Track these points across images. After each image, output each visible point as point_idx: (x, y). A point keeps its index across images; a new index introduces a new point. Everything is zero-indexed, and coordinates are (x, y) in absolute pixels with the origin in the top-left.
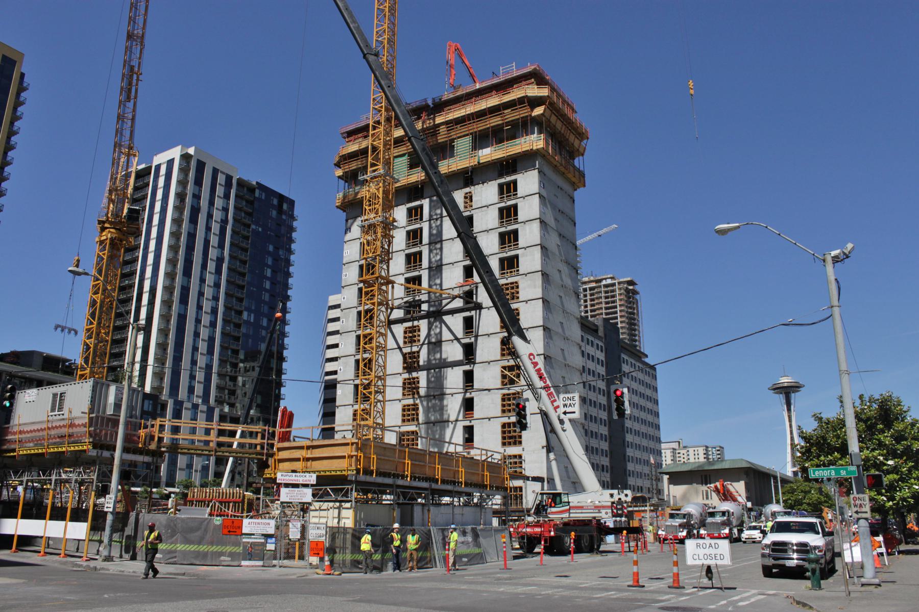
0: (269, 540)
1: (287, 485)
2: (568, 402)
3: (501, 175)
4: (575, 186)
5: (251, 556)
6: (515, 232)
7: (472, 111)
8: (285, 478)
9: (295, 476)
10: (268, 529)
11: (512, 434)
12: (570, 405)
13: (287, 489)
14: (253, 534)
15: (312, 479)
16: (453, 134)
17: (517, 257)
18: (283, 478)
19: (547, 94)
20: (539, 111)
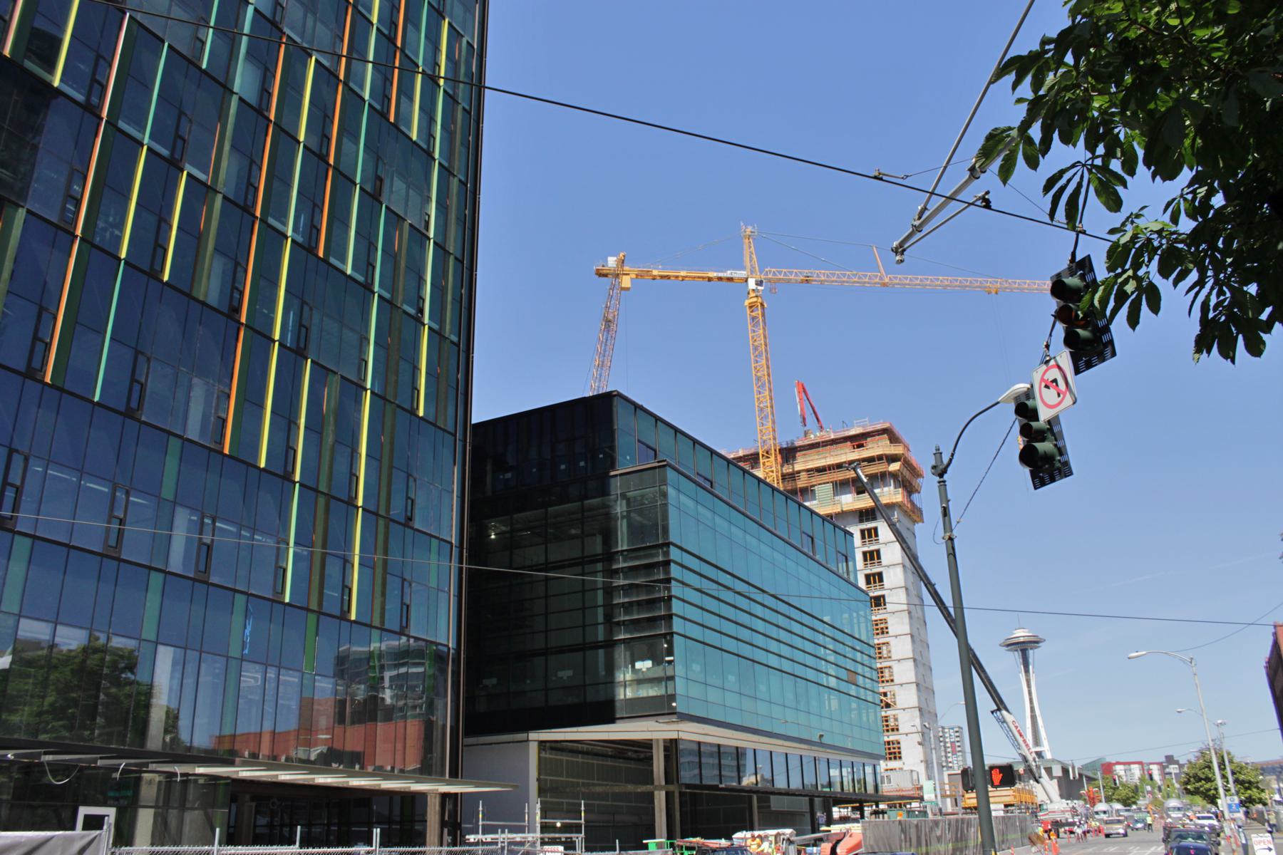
3: (861, 521)
4: (914, 522)
6: (880, 575)
7: (832, 462)
11: (892, 750)
16: (813, 481)
17: (883, 596)
19: (901, 452)
20: (895, 467)
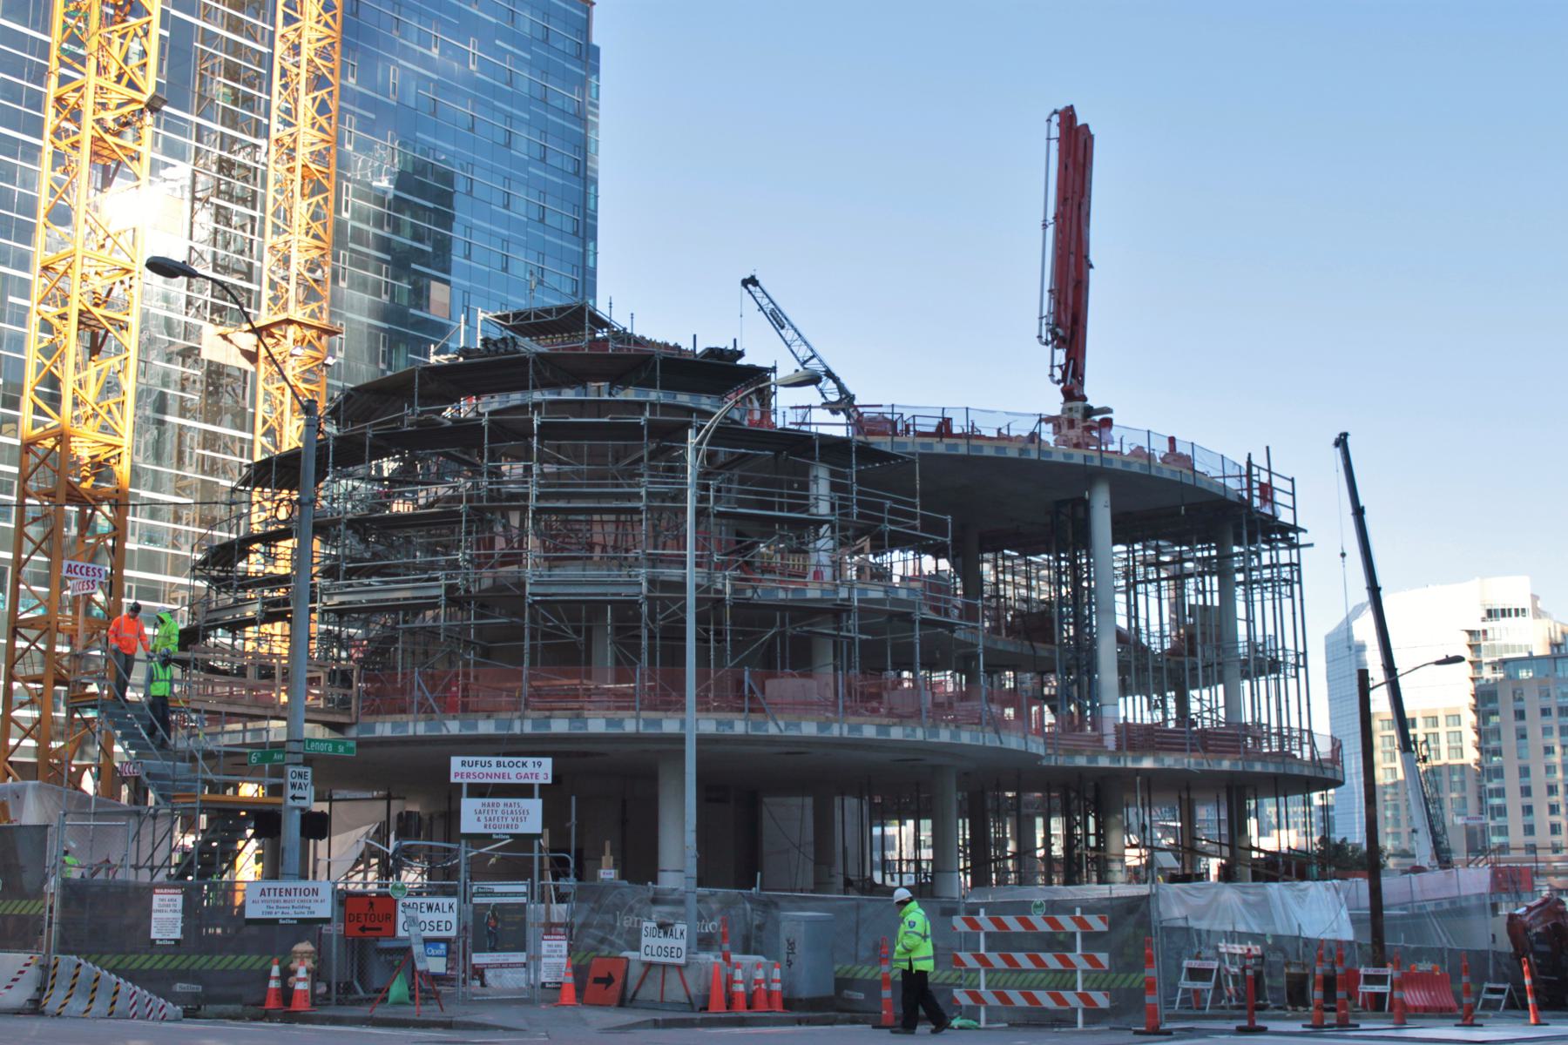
1: (478, 791)
8: (471, 770)
9: (498, 764)
15: (541, 770)
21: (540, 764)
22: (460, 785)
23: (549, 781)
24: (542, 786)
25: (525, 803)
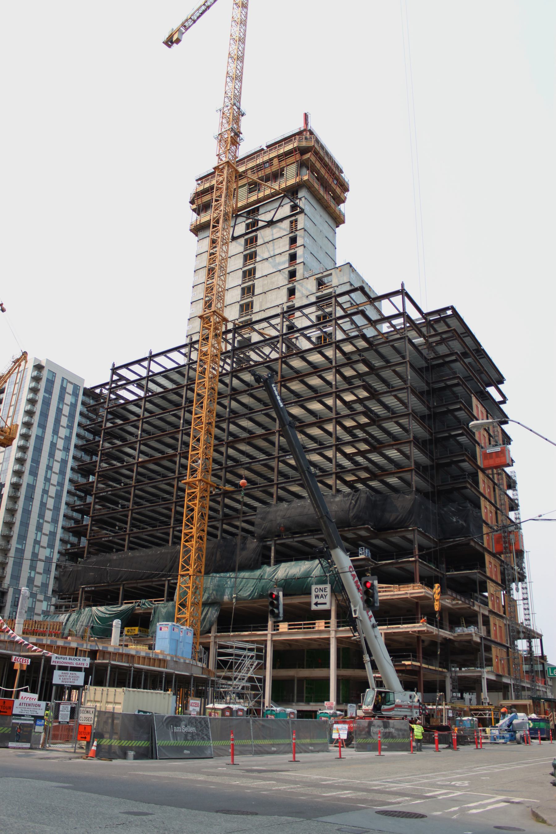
0: (38, 722)
1: (62, 668)
2: (320, 593)
5: (19, 737)
9: (70, 659)
10: (38, 711)
12: (322, 596)
13: (61, 672)
14: (23, 716)
18: (57, 660)
21: (85, 660)
22: (55, 666)
23: (88, 667)
24: (85, 668)
25: (78, 673)
